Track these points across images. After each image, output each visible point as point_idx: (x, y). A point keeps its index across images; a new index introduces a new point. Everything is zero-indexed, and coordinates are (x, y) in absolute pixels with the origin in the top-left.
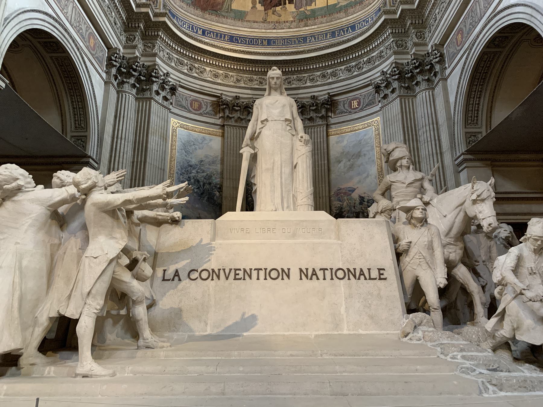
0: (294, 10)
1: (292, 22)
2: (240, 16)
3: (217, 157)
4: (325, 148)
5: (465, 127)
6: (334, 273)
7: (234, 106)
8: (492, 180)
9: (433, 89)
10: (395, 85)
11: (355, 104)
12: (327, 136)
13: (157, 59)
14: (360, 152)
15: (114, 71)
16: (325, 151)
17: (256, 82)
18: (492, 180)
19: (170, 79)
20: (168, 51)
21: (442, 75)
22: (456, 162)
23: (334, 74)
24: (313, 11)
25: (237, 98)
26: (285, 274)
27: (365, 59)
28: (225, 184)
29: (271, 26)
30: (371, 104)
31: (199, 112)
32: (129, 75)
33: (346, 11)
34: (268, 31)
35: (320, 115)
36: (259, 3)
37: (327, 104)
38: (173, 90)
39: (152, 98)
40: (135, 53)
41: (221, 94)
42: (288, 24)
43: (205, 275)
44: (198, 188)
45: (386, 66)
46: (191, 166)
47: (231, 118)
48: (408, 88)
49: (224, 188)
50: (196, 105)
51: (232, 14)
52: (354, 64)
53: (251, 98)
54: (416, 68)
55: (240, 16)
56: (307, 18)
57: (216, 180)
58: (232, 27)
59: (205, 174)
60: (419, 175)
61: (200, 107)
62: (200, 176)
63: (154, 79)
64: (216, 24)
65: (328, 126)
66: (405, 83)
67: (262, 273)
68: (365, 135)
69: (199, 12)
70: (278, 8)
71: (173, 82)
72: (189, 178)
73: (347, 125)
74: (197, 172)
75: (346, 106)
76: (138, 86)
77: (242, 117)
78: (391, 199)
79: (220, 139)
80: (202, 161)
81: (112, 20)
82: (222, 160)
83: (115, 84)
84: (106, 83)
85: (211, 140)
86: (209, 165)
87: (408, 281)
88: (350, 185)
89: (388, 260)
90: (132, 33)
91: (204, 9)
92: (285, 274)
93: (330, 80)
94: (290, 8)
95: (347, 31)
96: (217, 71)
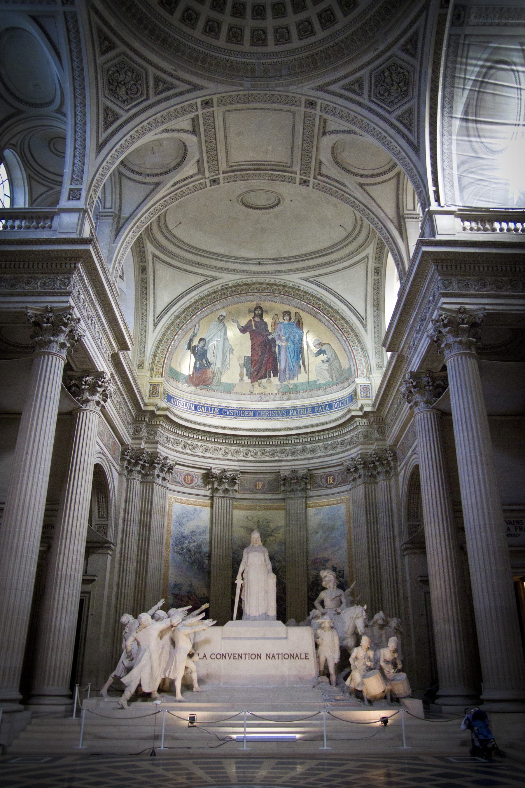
0: (278, 383)
1: (276, 394)
2: (229, 389)
3: (207, 527)
4: (304, 519)
5: (408, 521)
6: (283, 656)
7: (222, 478)
8: (365, 607)
9: (390, 479)
10: (361, 472)
11: (330, 479)
12: (306, 508)
13: (159, 446)
14: (334, 525)
15: (125, 463)
16: (304, 522)
17: (242, 454)
18: (365, 607)
19: (168, 461)
20: (167, 434)
21: (395, 472)
22: (403, 548)
23: (313, 451)
24: (295, 385)
25: (224, 471)
26: (259, 656)
27: (339, 440)
28: (213, 554)
29: (257, 397)
30: (344, 482)
31: (191, 485)
32: (137, 464)
33: (325, 389)
34: (254, 403)
35: (300, 488)
36: (247, 375)
37: (306, 479)
38: (171, 468)
39: (154, 482)
40: (141, 444)
41: (211, 468)
42: (272, 396)
43: (219, 656)
44: (190, 557)
45: (354, 452)
46: (184, 537)
47: (219, 490)
48: (372, 476)
49: (213, 557)
50: (189, 479)
51: (221, 388)
52: (329, 442)
53: (237, 470)
54: (378, 461)
55: (229, 389)
56: (290, 391)
57: (205, 549)
58: (221, 400)
59: (195, 544)
60: (340, 592)
61: (192, 480)
62: (192, 546)
63: (156, 465)
64: (207, 398)
65: (306, 497)
66: (368, 472)
67: (247, 656)
68: (339, 510)
69: (192, 388)
70: (264, 381)
71: (170, 462)
72: (182, 548)
73: (323, 499)
74: (189, 542)
75: (323, 480)
76: (143, 472)
77: (229, 488)
78: (323, 607)
79: (209, 509)
80: (193, 532)
81: (126, 422)
82: (211, 529)
83: (125, 472)
84: (120, 474)
85: (201, 511)
86: (200, 535)
87: (322, 660)
88: (325, 555)
89: (310, 648)
90: (138, 425)
91: (196, 385)
92: (259, 656)
93: (309, 456)
94: (275, 380)
95: (325, 408)
96: (207, 445)
